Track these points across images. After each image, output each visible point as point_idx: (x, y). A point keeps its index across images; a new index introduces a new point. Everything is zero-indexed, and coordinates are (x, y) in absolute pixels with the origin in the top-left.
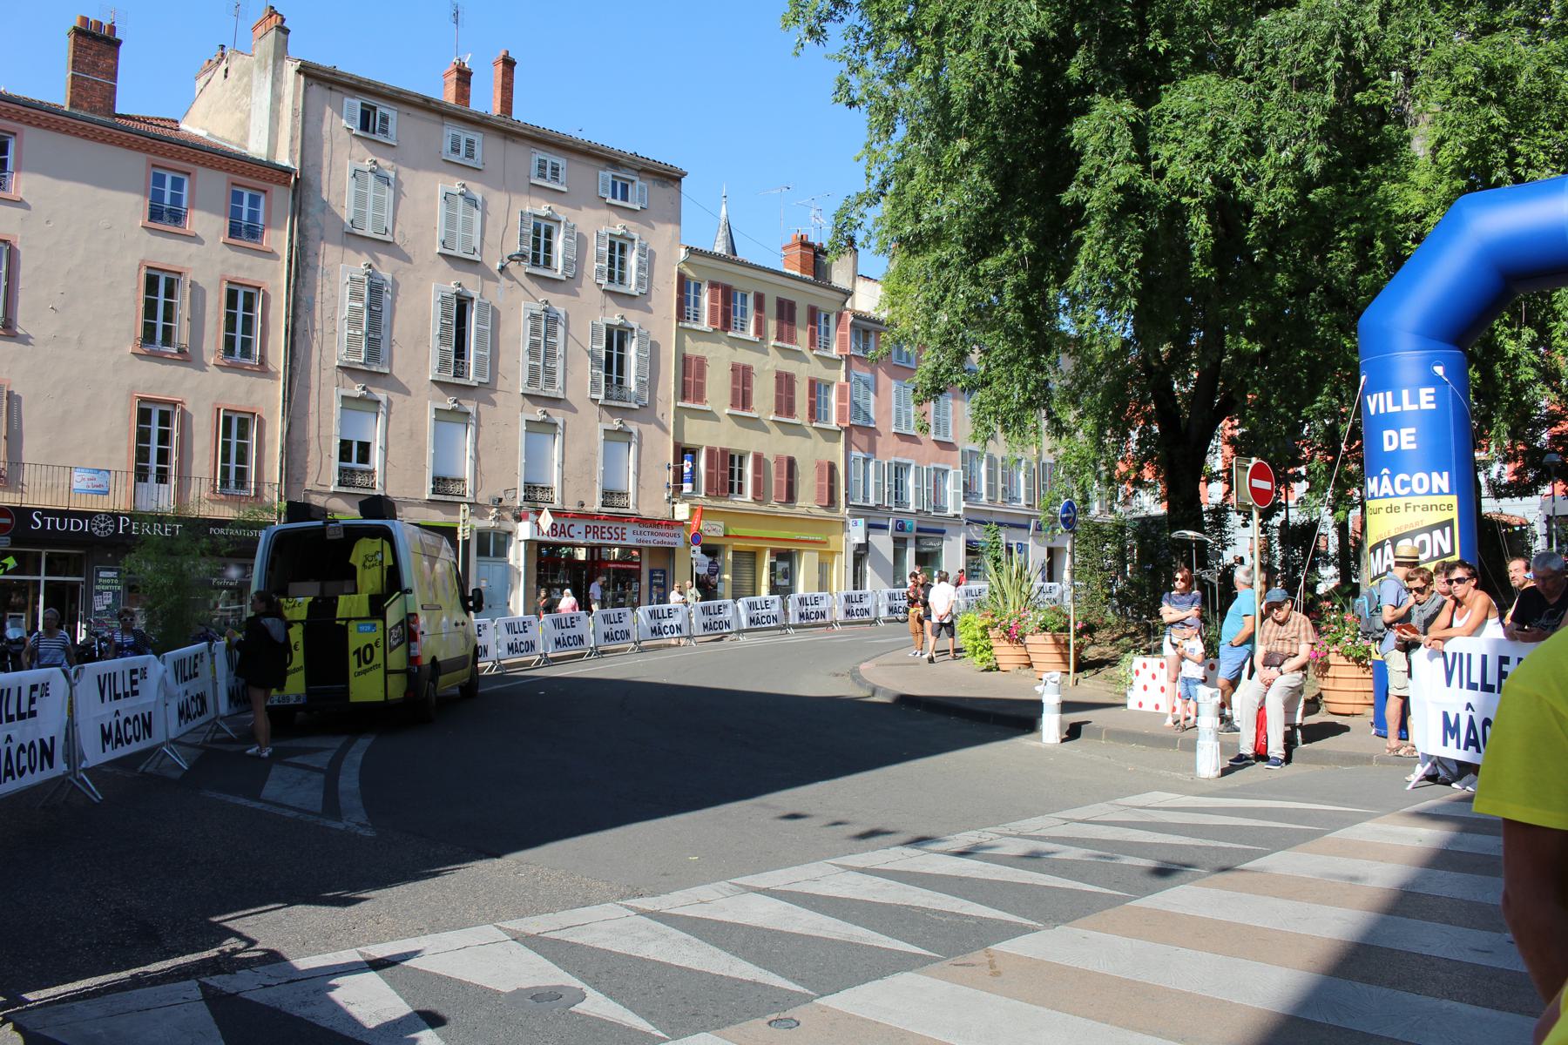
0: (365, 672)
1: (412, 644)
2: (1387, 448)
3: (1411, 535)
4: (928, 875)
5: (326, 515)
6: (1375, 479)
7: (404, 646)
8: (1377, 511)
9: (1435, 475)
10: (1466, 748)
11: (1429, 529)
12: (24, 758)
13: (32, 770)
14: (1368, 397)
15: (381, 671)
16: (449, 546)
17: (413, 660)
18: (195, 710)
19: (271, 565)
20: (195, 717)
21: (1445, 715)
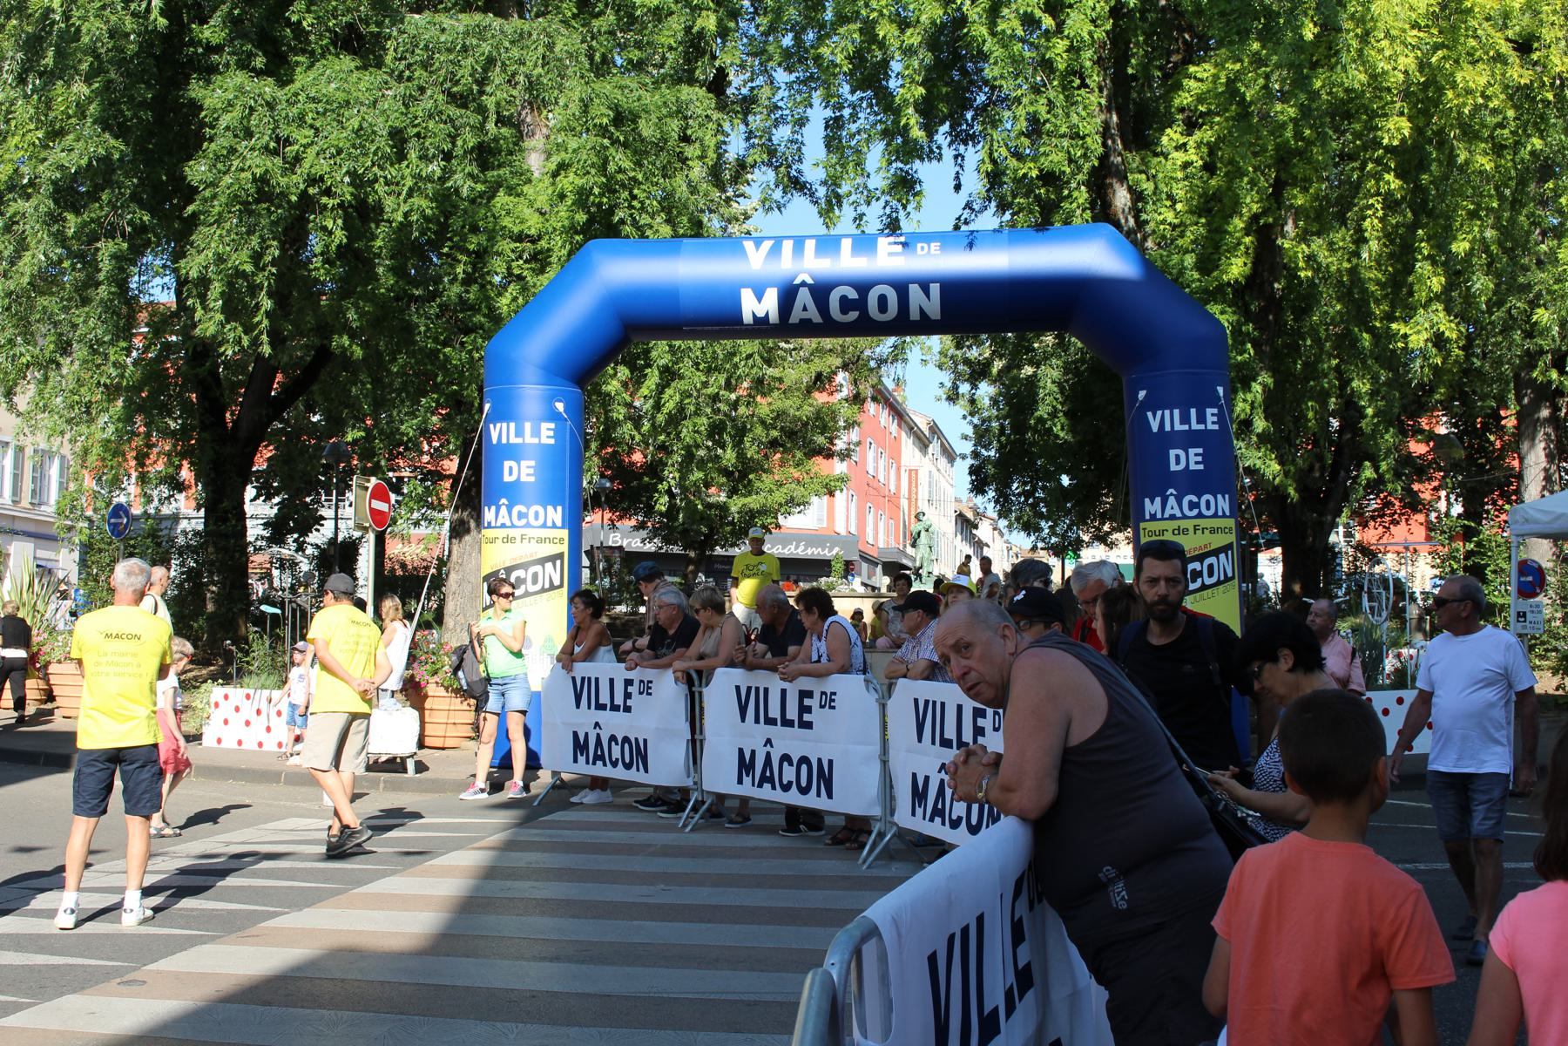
2: (507, 478)
3: (524, 566)
6: (493, 508)
8: (493, 541)
9: (550, 508)
10: (594, 763)
11: (542, 561)
14: (491, 426)
21: (575, 734)
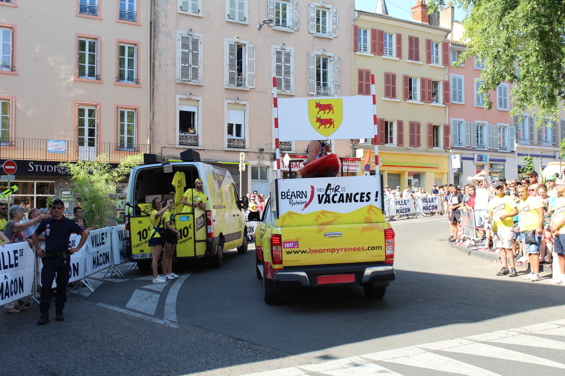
0: (184, 241)
1: (209, 227)
4: (472, 356)
5: (164, 160)
7: (204, 227)
12: (13, 286)
13: (16, 293)
15: (192, 240)
16: (230, 175)
17: (209, 235)
18: (101, 261)
19: (137, 187)
20: (101, 264)
